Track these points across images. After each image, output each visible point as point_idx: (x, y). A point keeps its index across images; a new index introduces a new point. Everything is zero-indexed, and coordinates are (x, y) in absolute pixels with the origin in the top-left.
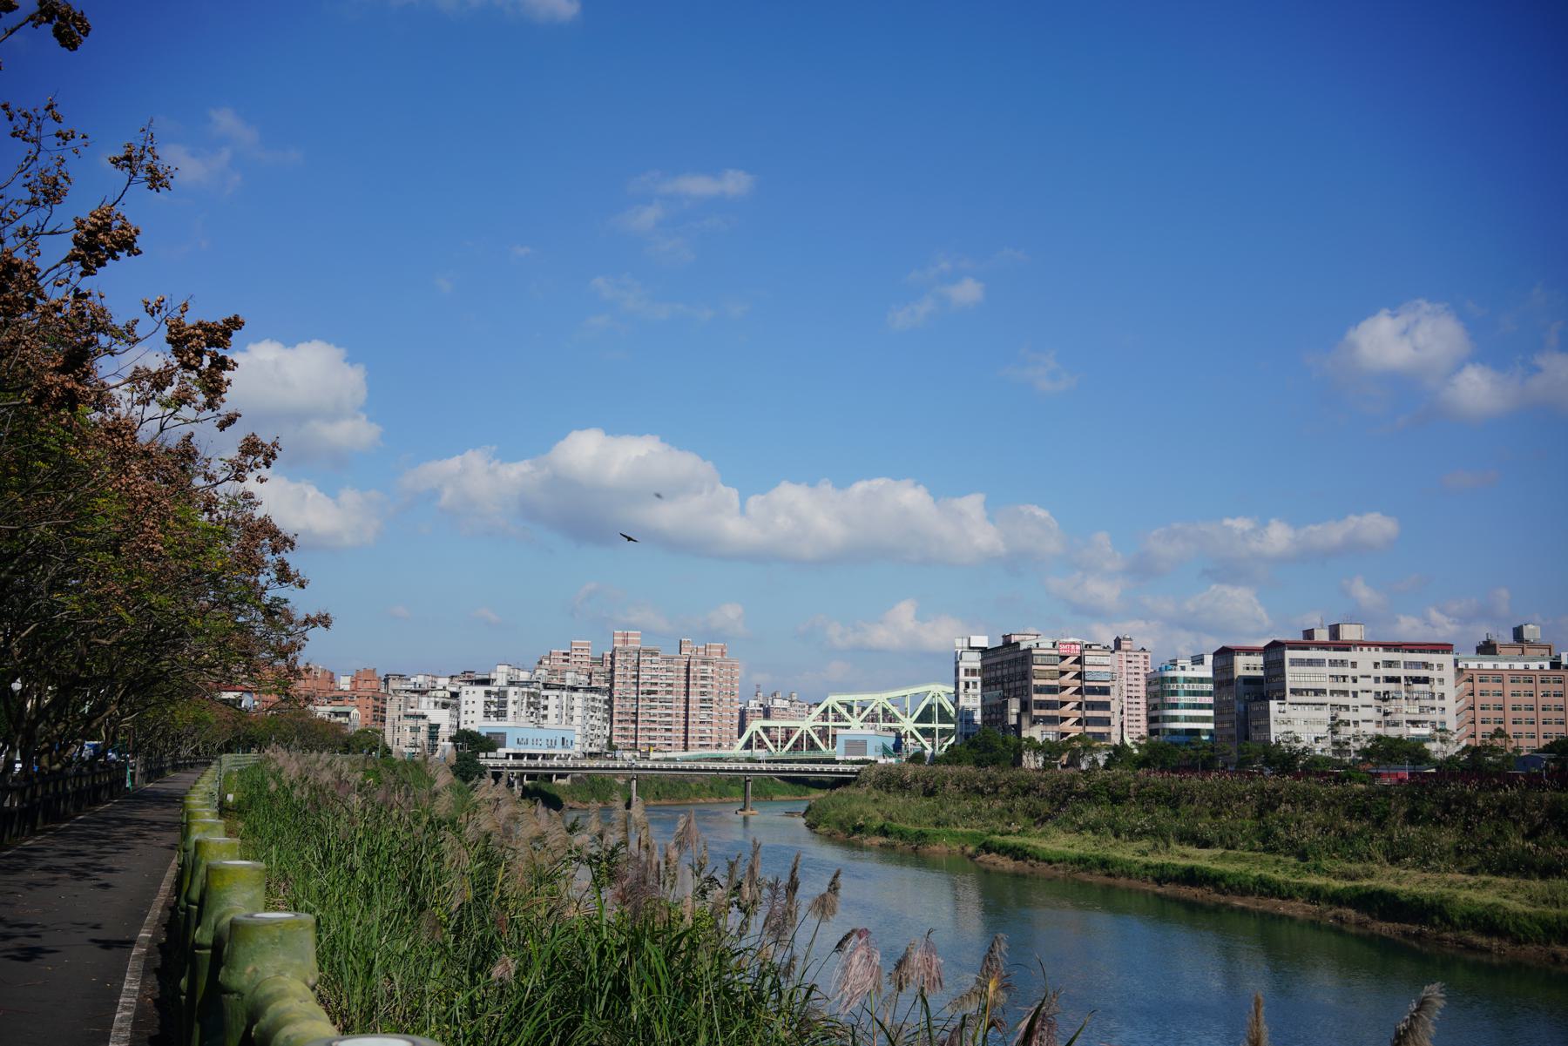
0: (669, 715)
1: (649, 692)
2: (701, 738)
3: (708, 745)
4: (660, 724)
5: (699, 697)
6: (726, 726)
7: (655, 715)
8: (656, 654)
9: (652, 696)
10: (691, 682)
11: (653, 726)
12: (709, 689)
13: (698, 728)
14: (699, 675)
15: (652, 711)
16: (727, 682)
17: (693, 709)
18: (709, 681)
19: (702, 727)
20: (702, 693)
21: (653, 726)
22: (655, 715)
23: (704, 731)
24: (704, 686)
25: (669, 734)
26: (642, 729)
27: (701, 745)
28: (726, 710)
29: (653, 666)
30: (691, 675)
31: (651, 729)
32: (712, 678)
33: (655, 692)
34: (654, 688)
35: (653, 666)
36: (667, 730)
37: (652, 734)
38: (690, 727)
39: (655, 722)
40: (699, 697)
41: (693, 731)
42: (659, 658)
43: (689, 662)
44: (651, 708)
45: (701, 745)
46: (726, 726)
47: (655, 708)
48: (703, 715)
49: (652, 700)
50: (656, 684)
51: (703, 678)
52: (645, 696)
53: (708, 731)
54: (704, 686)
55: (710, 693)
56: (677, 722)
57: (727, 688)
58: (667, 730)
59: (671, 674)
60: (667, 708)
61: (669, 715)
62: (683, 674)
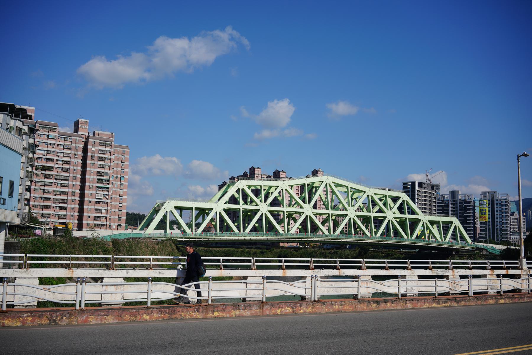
0: (64, 193)
1: (44, 168)
2: (97, 218)
3: (102, 225)
4: (55, 201)
5: (96, 177)
6: (115, 207)
7: (49, 192)
8: (54, 130)
9: (47, 172)
10: (89, 162)
11: (46, 203)
12: (107, 170)
13: (93, 207)
14: (97, 155)
15: (47, 188)
16: (117, 167)
17: (90, 189)
18: (107, 163)
19: (98, 207)
20: (99, 174)
21: (46, 203)
22: (49, 192)
23: (99, 211)
24: (101, 167)
25: (63, 212)
26: (35, 206)
27: (97, 225)
28: (115, 193)
29: (50, 141)
30: (89, 154)
31: (44, 207)
32: (110, 159)
33: (51, 169)
34: (49, 164)
35: (50, 141)
36: (61, 208)
37: (45, 211)
38: (85, 207)
39: (48, 199)
40: (96, 177)
41: (89, 210)
42: (55, 134)
43: (86, 144)
44: (46, 184)
45: (97, 225)
46: (115, 207)
47: (50, 185)
48: (100, 195)
49: (47, 176)
50: (52, 160)
51: (101, 159)
52: (39, 172)
53: (103, 211)
54: (101, 167)
55: (107, 174)
56: (73, 200)
57: (117, 172)
58: (61, 208)
59: (69, 151)
60: (62, 186)
61: (64, 193)
62: (80, 153)
